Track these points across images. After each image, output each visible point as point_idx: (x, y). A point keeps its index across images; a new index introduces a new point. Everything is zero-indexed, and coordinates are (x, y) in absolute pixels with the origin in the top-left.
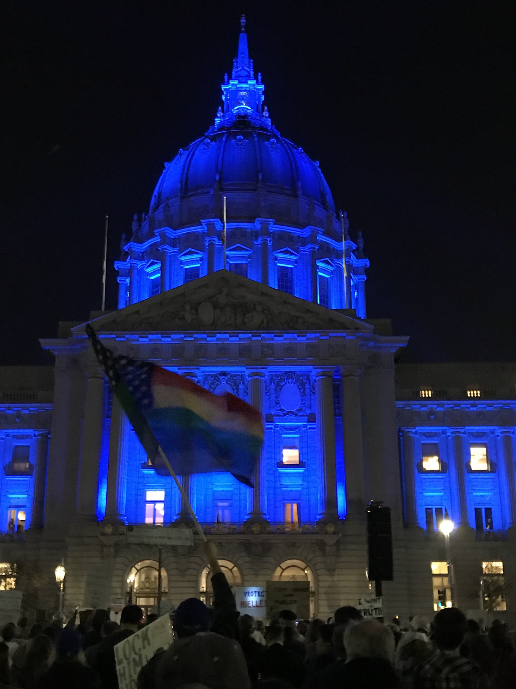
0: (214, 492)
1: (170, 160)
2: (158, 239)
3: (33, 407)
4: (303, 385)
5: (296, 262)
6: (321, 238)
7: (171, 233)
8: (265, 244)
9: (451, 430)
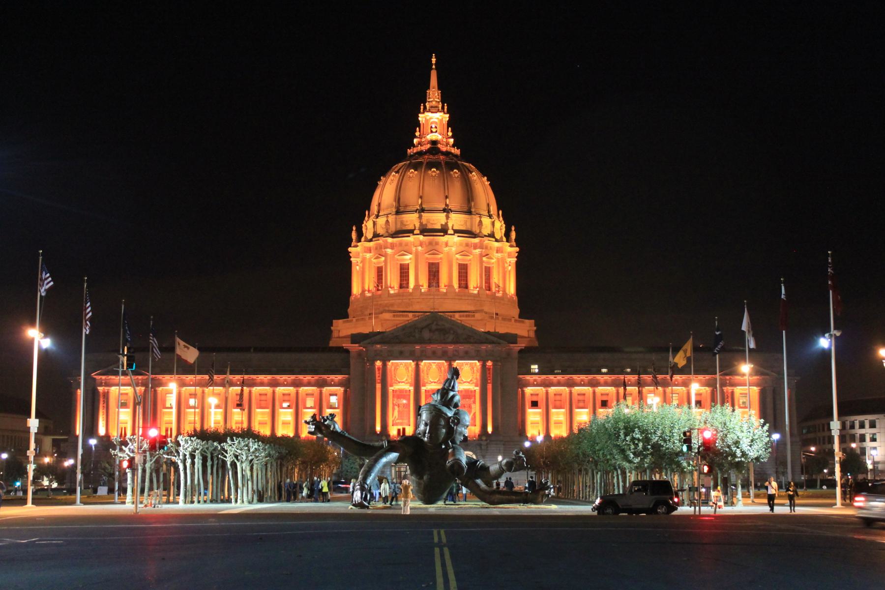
1: (384, 175)
3: (340, 377)
7: (390, 240)
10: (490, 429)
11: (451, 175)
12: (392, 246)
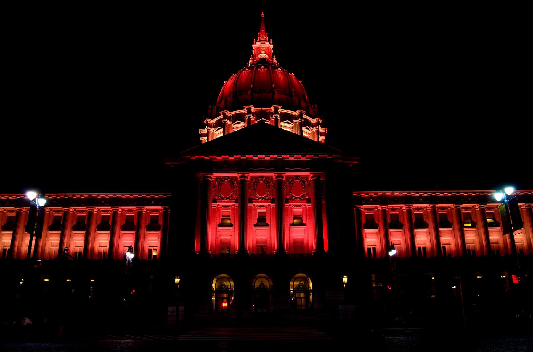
0: (257, 240)
1: (227, 80)
2: (221, 117)
4: (304, 182)
5: (292, 128)
6: (304, 116)
7: (228, 114)
8: (276, 119)
9: (381, 207)
10: (326, 248)
11: (276, 72)
12: (229, 118)
